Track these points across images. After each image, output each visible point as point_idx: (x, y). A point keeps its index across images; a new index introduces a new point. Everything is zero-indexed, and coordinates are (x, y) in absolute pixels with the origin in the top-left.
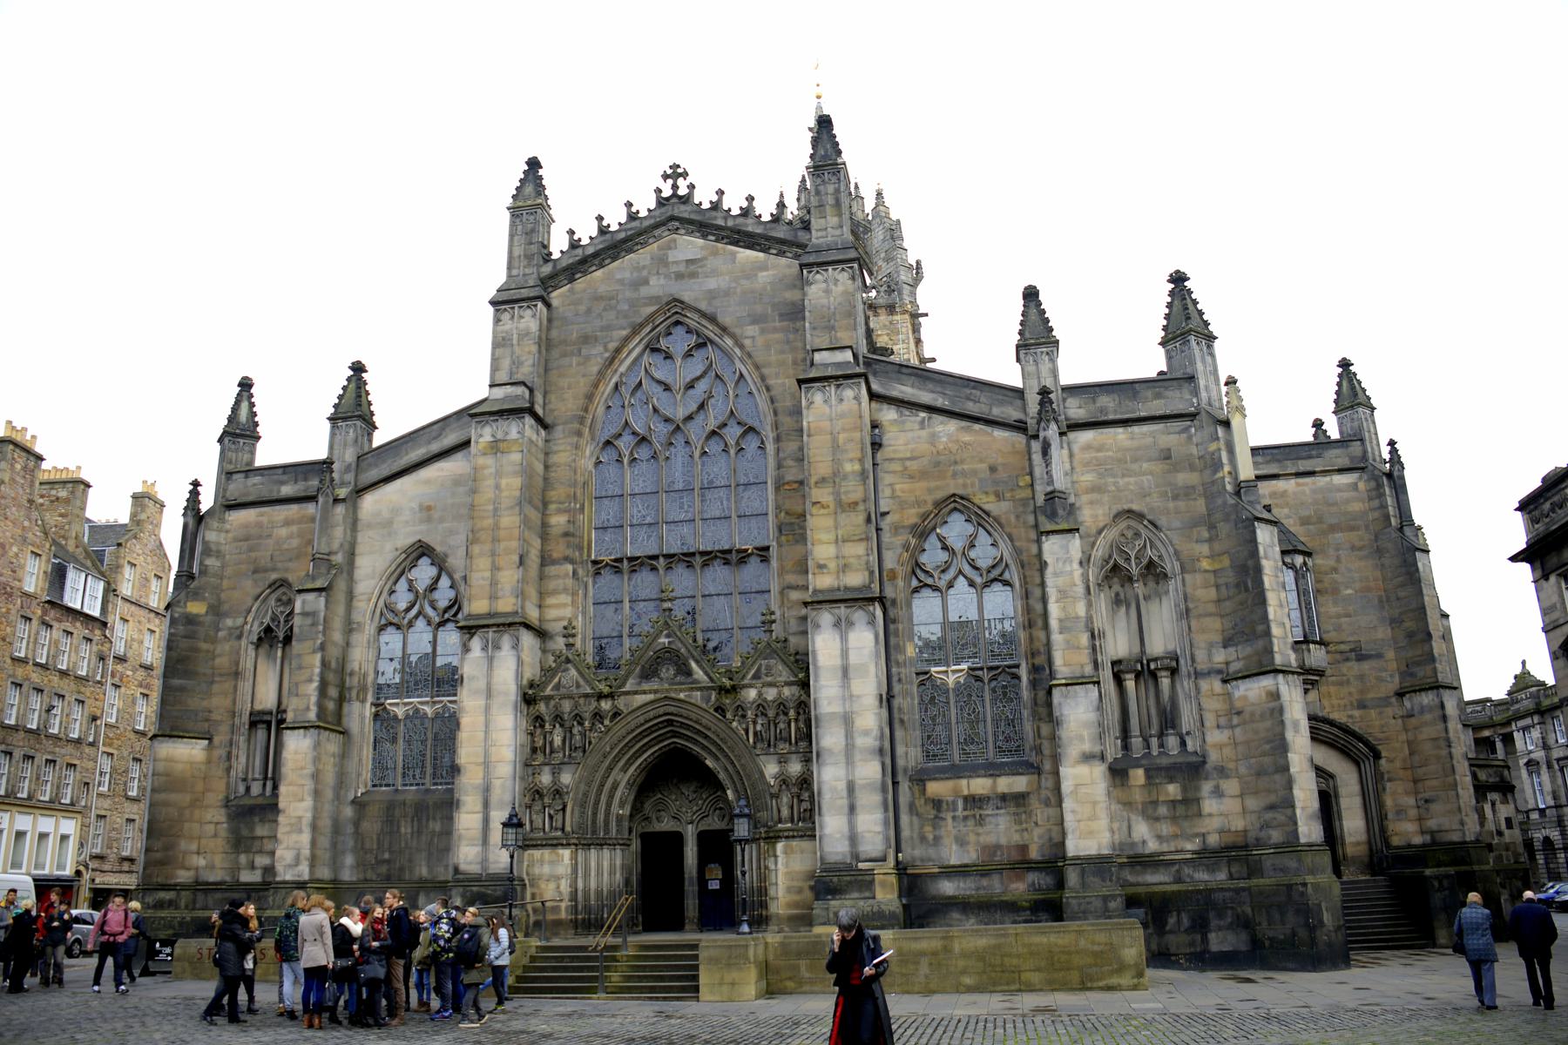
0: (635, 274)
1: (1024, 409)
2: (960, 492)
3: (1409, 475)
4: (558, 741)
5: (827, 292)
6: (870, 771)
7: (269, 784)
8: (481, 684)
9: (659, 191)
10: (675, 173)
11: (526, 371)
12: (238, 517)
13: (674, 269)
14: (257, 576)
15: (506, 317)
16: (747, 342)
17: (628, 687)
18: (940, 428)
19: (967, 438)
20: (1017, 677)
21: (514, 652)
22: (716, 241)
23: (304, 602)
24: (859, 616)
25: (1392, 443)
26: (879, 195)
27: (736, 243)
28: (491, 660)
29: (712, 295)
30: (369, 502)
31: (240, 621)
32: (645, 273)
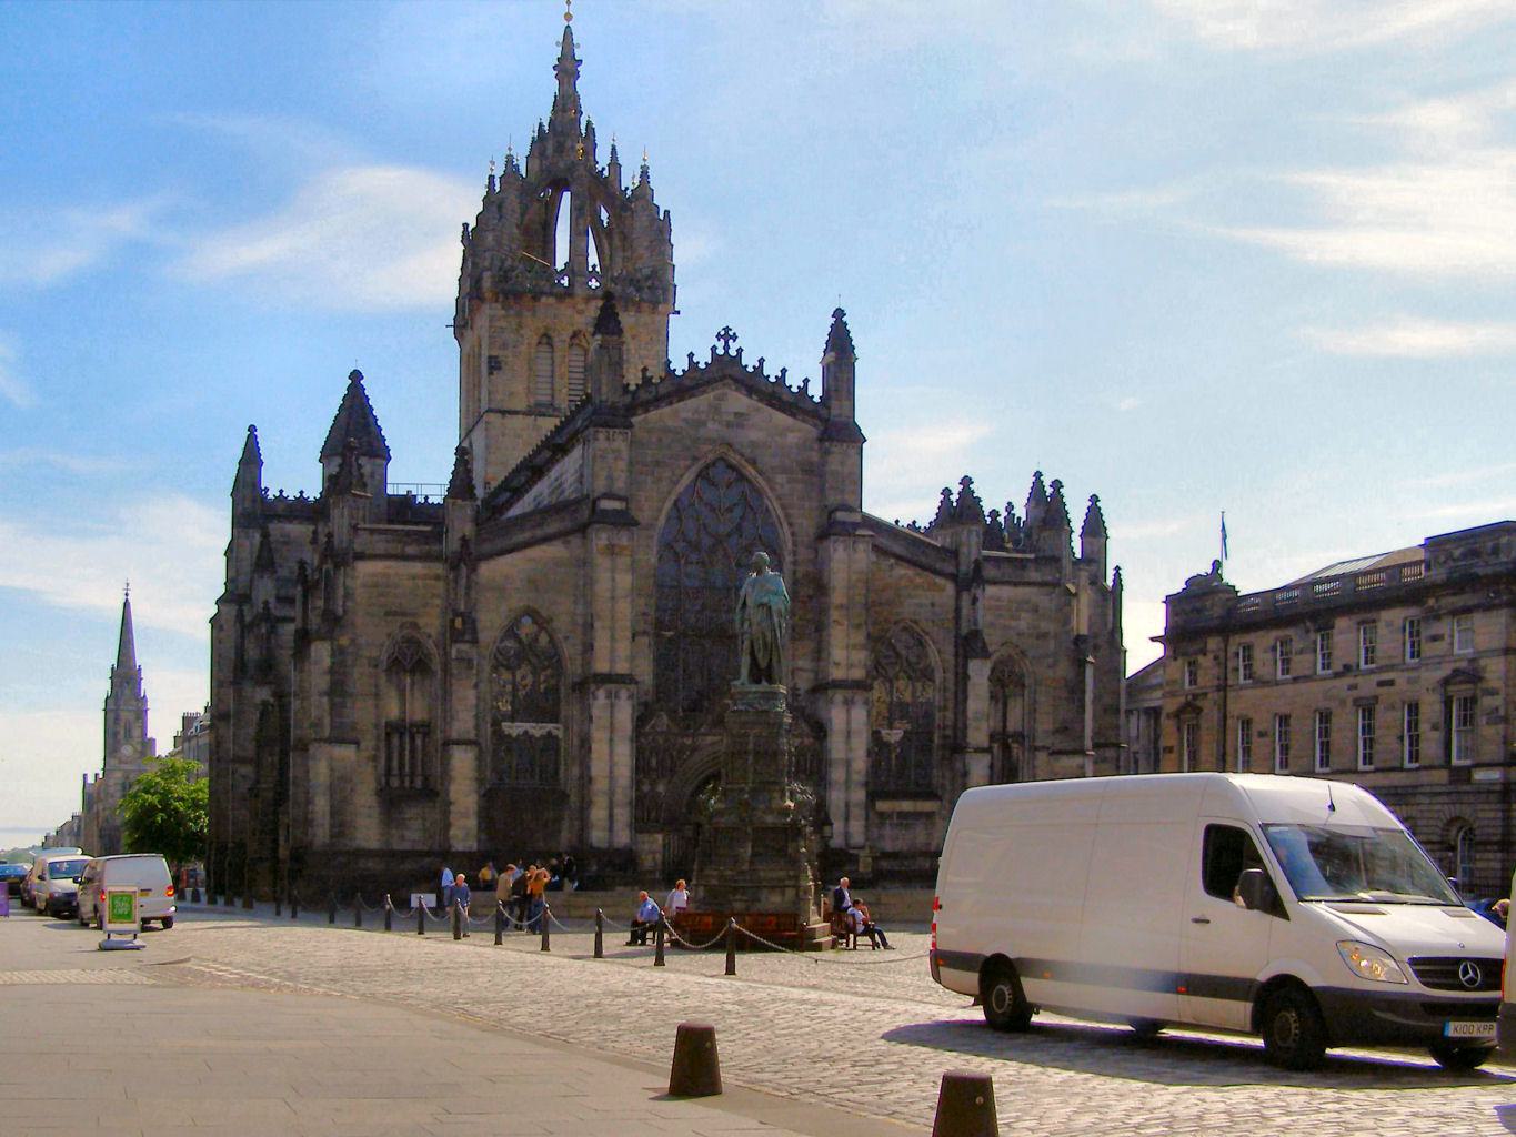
0: (696, 416)
1: (958, 566)
2: (913, 618)
3: (1124, 594)
4: (654, 762)
5: (842, 463)
6: (859, 795)
7: (407, 780)
8: (606, 721)
9: (714, 349)
10: (727, 335)
11: (620, 485)
12: (365, 569)
13: (725, 417)
14: (389, 618)
15: (601, 436)
16: (778, 487)
17: (702, 730)
18: (903, 572)
19: (918, 580)
20: (932, 741)
21: (630, 702)
22: (760, 400)
23: (458, 651)
24: (859, 697)
25: (1117, 569)
26: (645, 174)
27: (771, 405)
28: (612, 706)
29: (753, 444)
30: (487, 570)
31: (375, 653)
32: (703, 417)
